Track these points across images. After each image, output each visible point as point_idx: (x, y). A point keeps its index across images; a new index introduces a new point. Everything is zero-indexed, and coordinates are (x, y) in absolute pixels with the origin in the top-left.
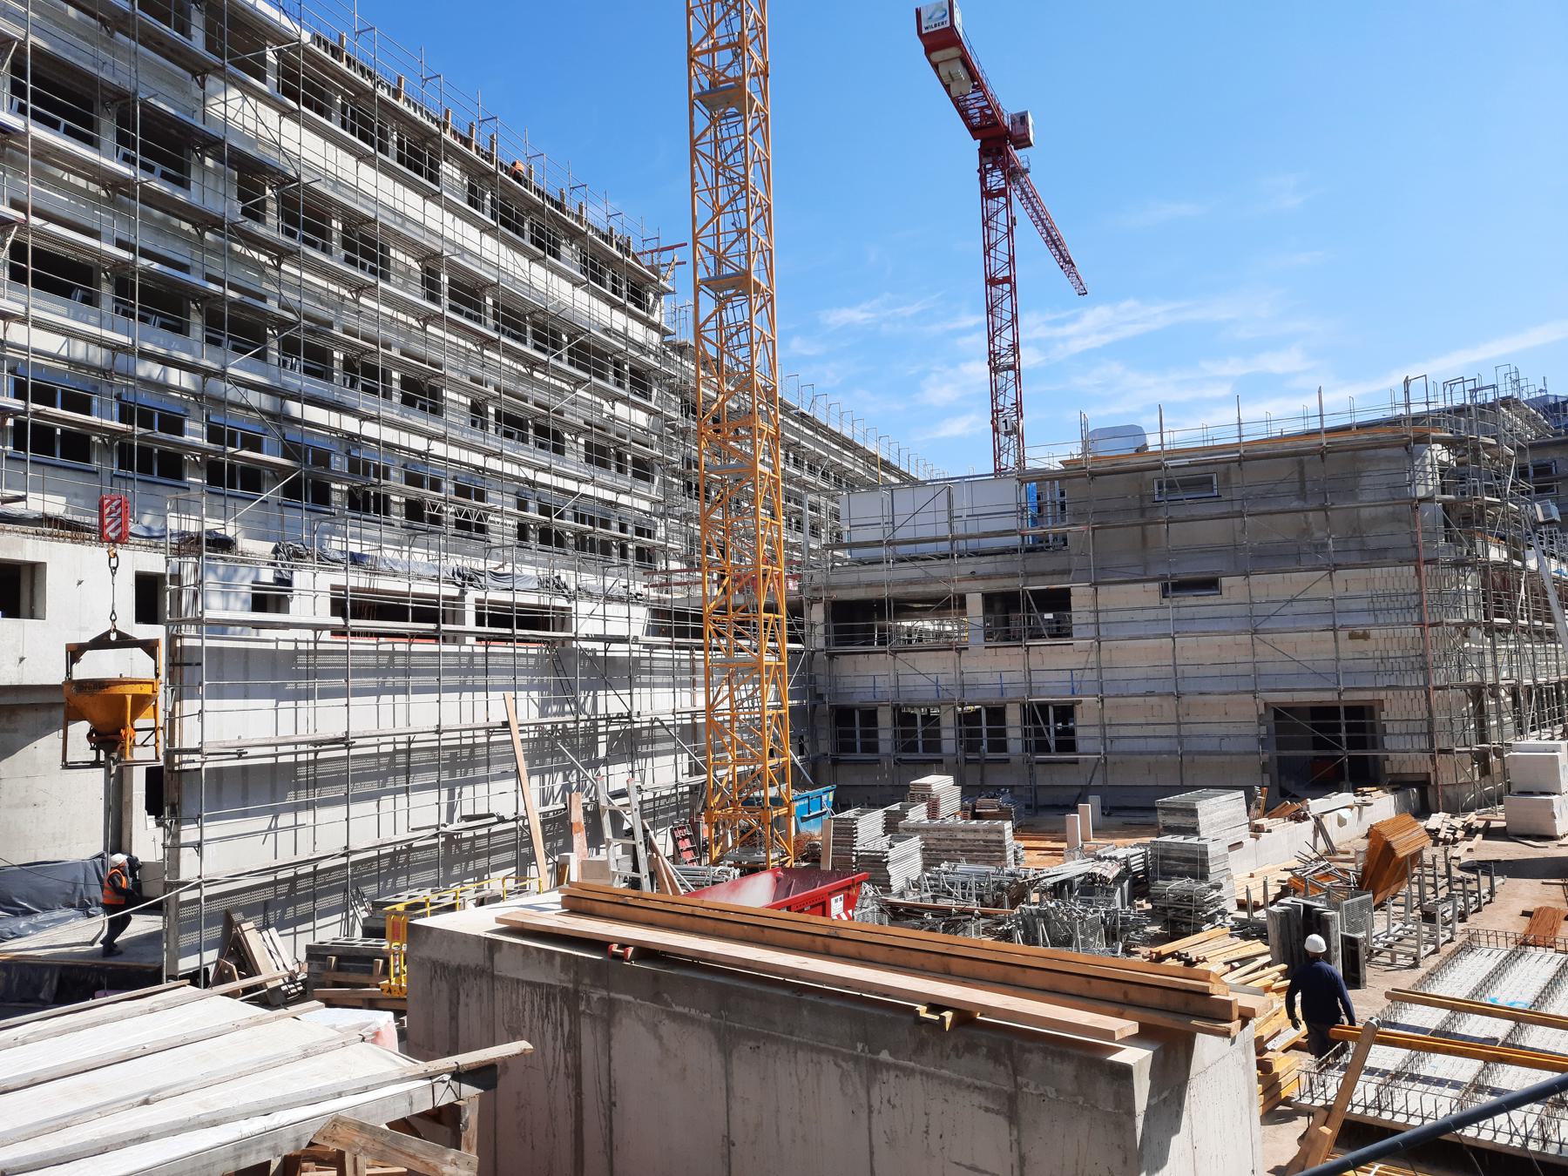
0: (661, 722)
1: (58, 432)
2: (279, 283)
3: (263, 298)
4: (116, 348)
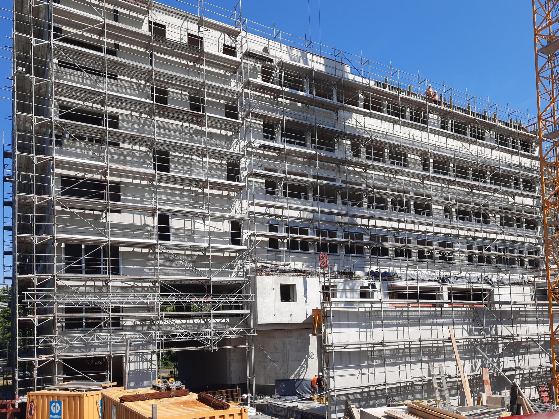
1: (299, 242)
2: (366, 177)
4: (313, 212)
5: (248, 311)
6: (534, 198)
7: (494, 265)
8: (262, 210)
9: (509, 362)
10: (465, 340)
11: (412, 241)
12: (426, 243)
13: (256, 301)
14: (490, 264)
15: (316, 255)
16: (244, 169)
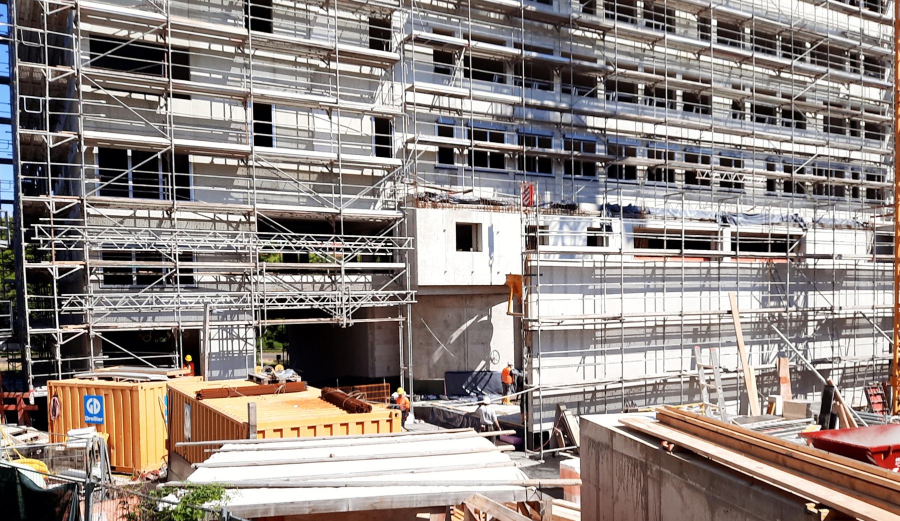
0: (863, 314)
1: (489, 154)
3: (594, 60)
4: (514, 105)
5: (402, 265)
6: (881, 87)
7: (808, 197)
8: (428, 99)
9: (822, 349)
10: (754, 315)
11: (676, 155)
12: (700, 159)
13: (416, 248)
14: (802, 195)
15: (516, 176)
16: (399, 30)
